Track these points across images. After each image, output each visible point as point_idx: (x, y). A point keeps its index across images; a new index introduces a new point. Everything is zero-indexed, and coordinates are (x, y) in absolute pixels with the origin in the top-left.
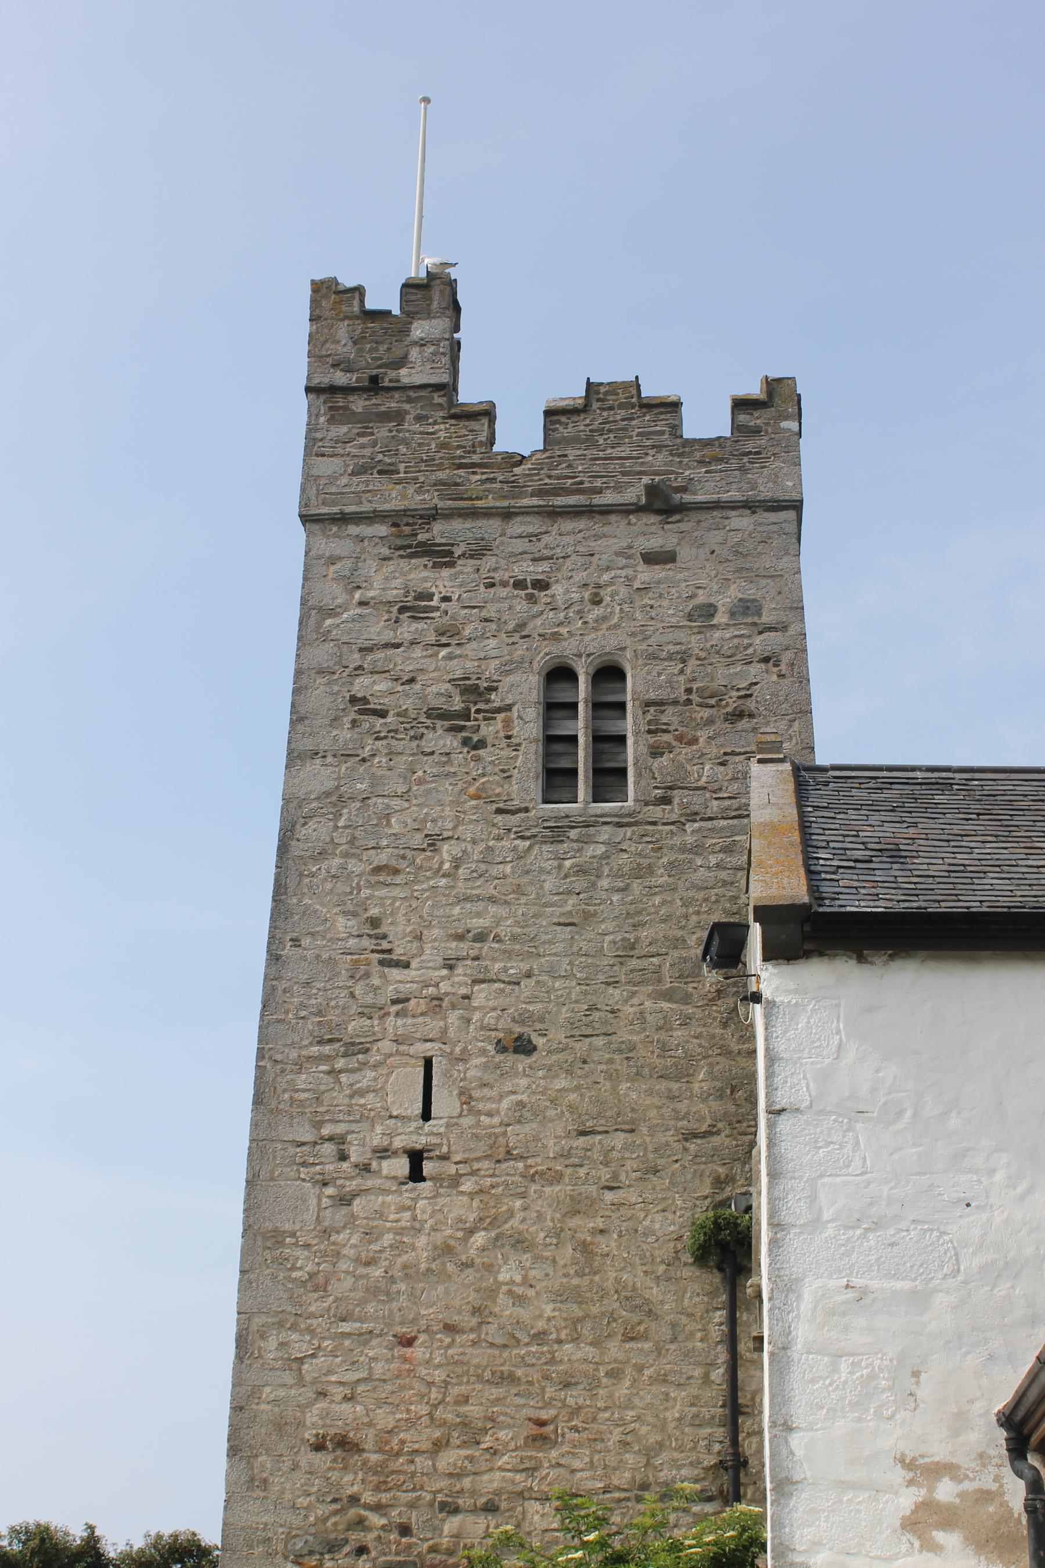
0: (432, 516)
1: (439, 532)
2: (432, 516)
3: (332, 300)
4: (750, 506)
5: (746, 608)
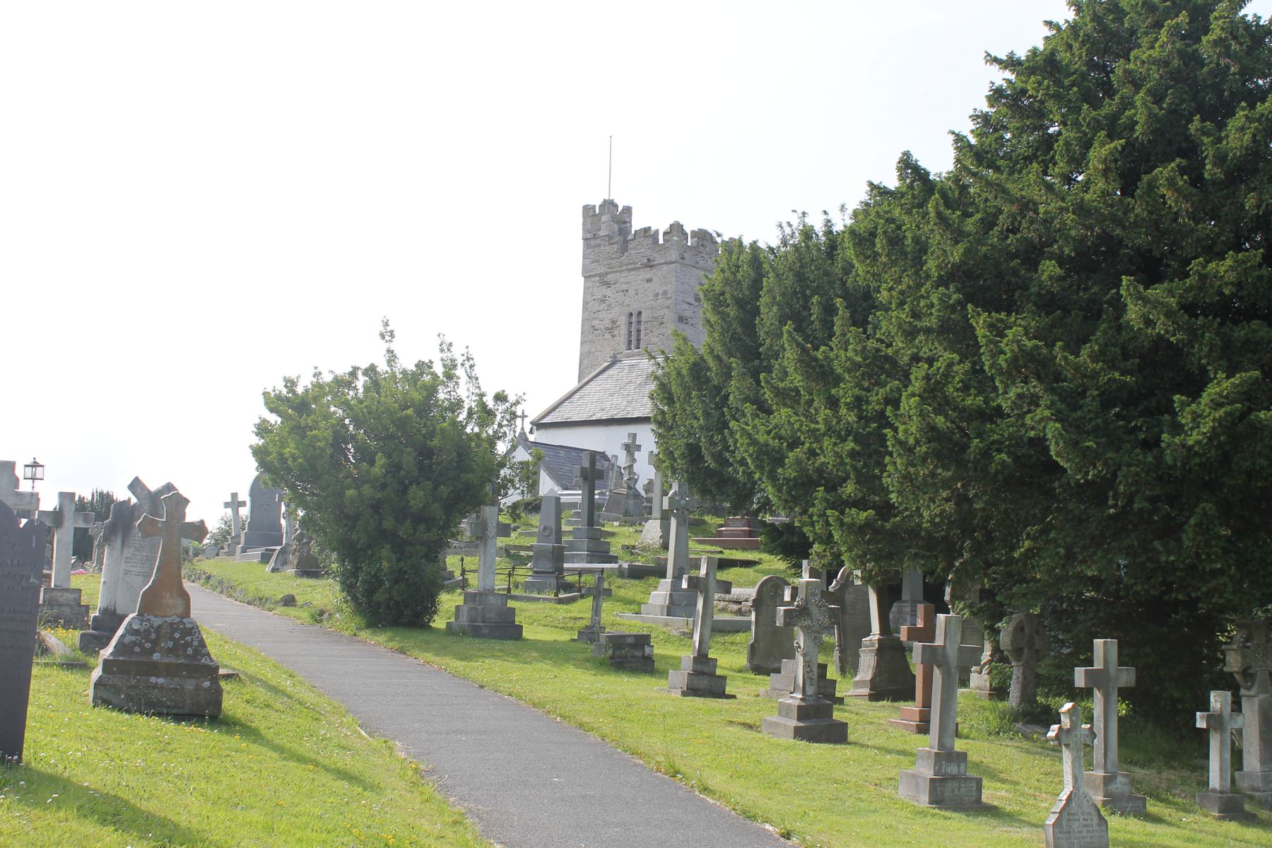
0: (607, 274)
1: (610, 277)
2: (607, 274)
3: (588, 210)
4: (666, 263)
5: (665, 293)
